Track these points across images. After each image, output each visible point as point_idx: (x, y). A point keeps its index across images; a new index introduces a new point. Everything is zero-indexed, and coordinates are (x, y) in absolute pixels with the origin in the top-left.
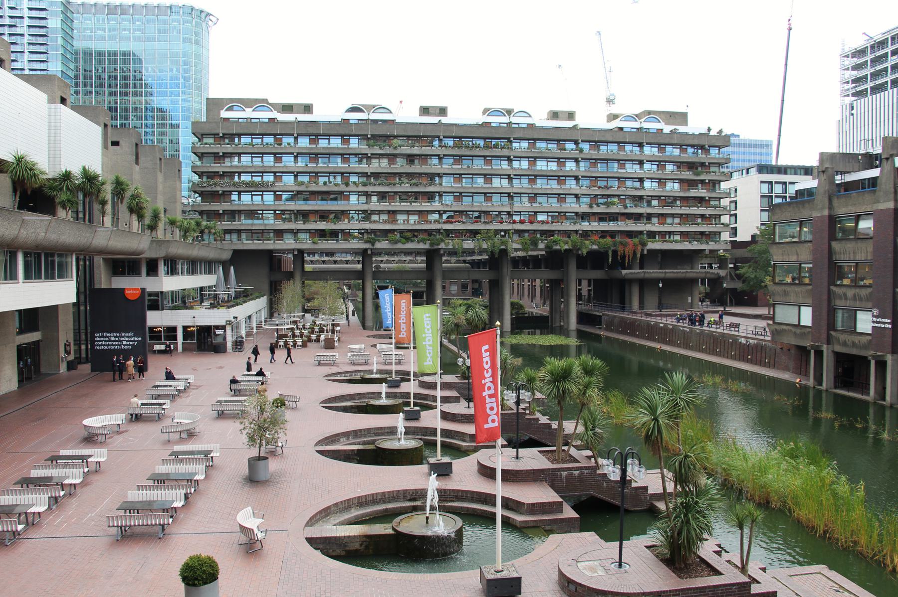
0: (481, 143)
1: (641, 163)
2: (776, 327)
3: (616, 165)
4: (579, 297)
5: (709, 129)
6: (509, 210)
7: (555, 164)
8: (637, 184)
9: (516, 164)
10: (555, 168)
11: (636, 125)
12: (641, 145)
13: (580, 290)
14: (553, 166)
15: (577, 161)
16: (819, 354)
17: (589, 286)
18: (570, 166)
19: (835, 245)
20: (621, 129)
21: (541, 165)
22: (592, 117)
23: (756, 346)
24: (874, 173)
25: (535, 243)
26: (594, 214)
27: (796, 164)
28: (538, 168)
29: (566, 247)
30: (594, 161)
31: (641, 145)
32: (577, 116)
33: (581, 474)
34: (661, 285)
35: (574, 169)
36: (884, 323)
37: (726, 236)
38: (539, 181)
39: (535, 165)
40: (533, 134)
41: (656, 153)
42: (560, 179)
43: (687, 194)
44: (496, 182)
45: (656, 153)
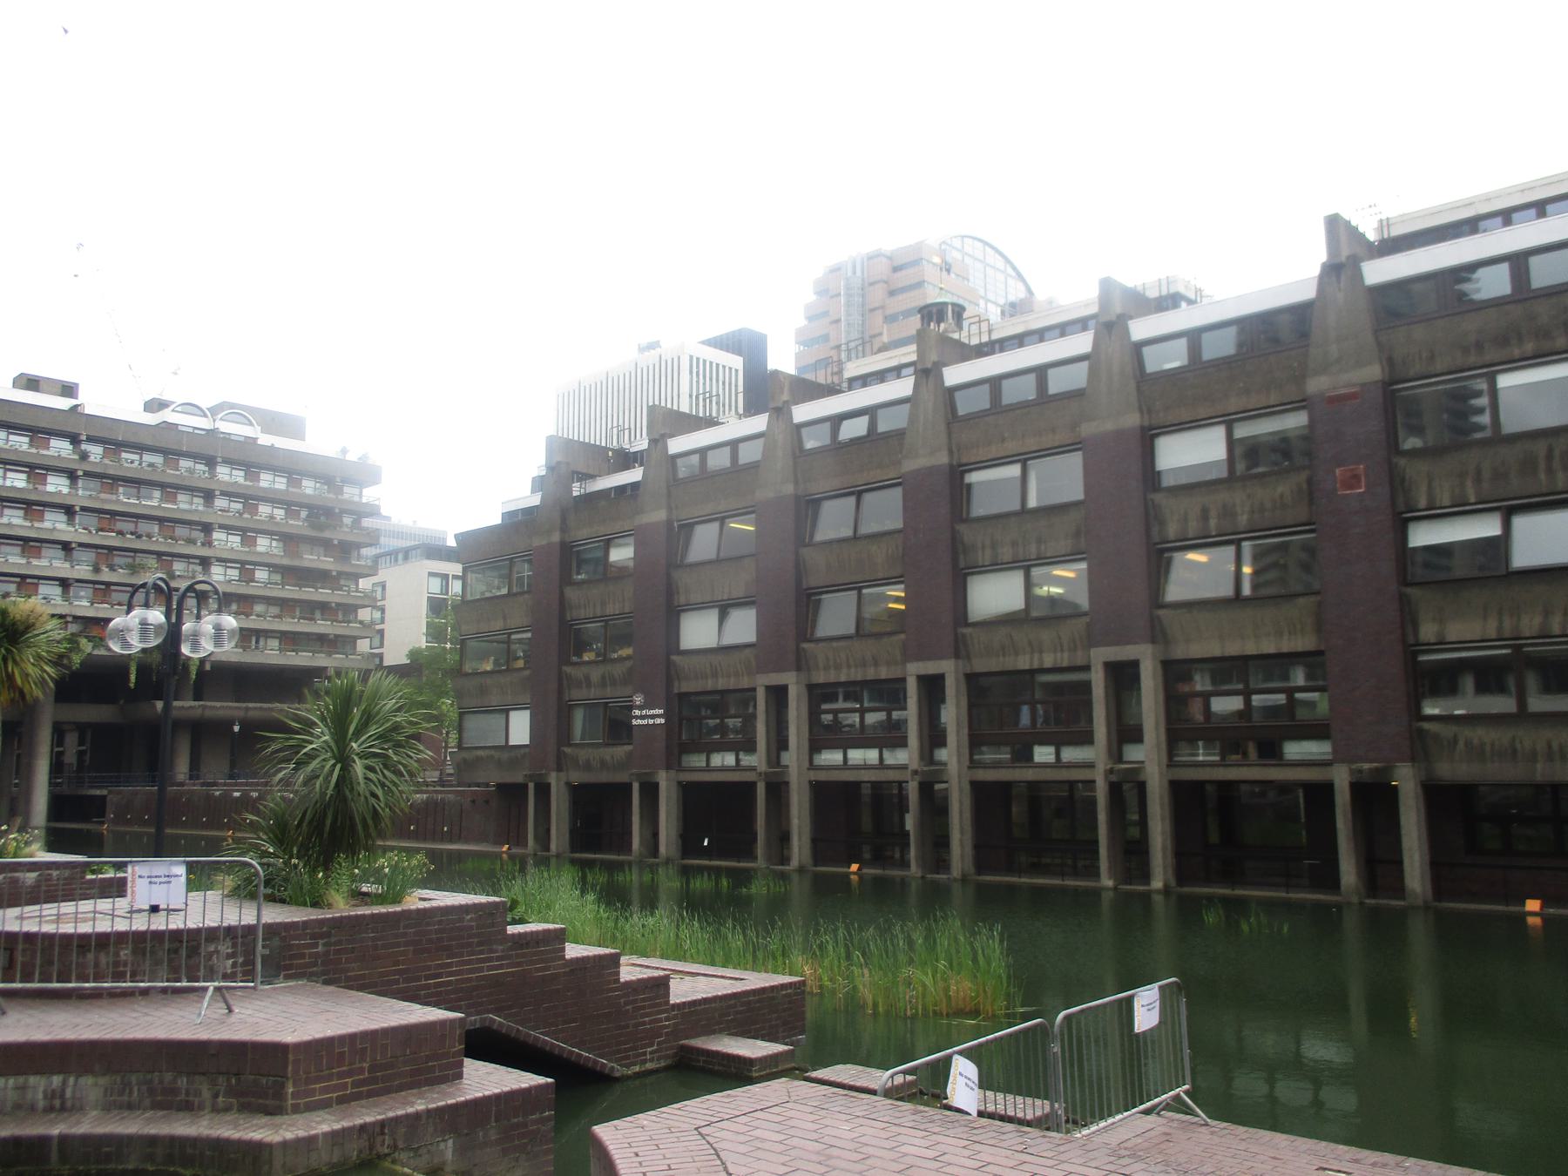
1: (208, 496)
2: (465, 755)
4: (57, 767)
5: (344, 451)
8: (199, 536)
11: (204, 423)
12: (211, 462)
13: (60, 754)
15: (72, 476)
16: (543, 790)
17: (81, 742)
18: (56, 485)
22: (111, 397)
23: (427, 803)
30: (111, 481)
31: (211, 462)
34: (236, 729)
35: (65, 490)
36: (653, 717)
37: (363, 646)
41: (241, 480)
43: (296, 563)
45: (241, 480)
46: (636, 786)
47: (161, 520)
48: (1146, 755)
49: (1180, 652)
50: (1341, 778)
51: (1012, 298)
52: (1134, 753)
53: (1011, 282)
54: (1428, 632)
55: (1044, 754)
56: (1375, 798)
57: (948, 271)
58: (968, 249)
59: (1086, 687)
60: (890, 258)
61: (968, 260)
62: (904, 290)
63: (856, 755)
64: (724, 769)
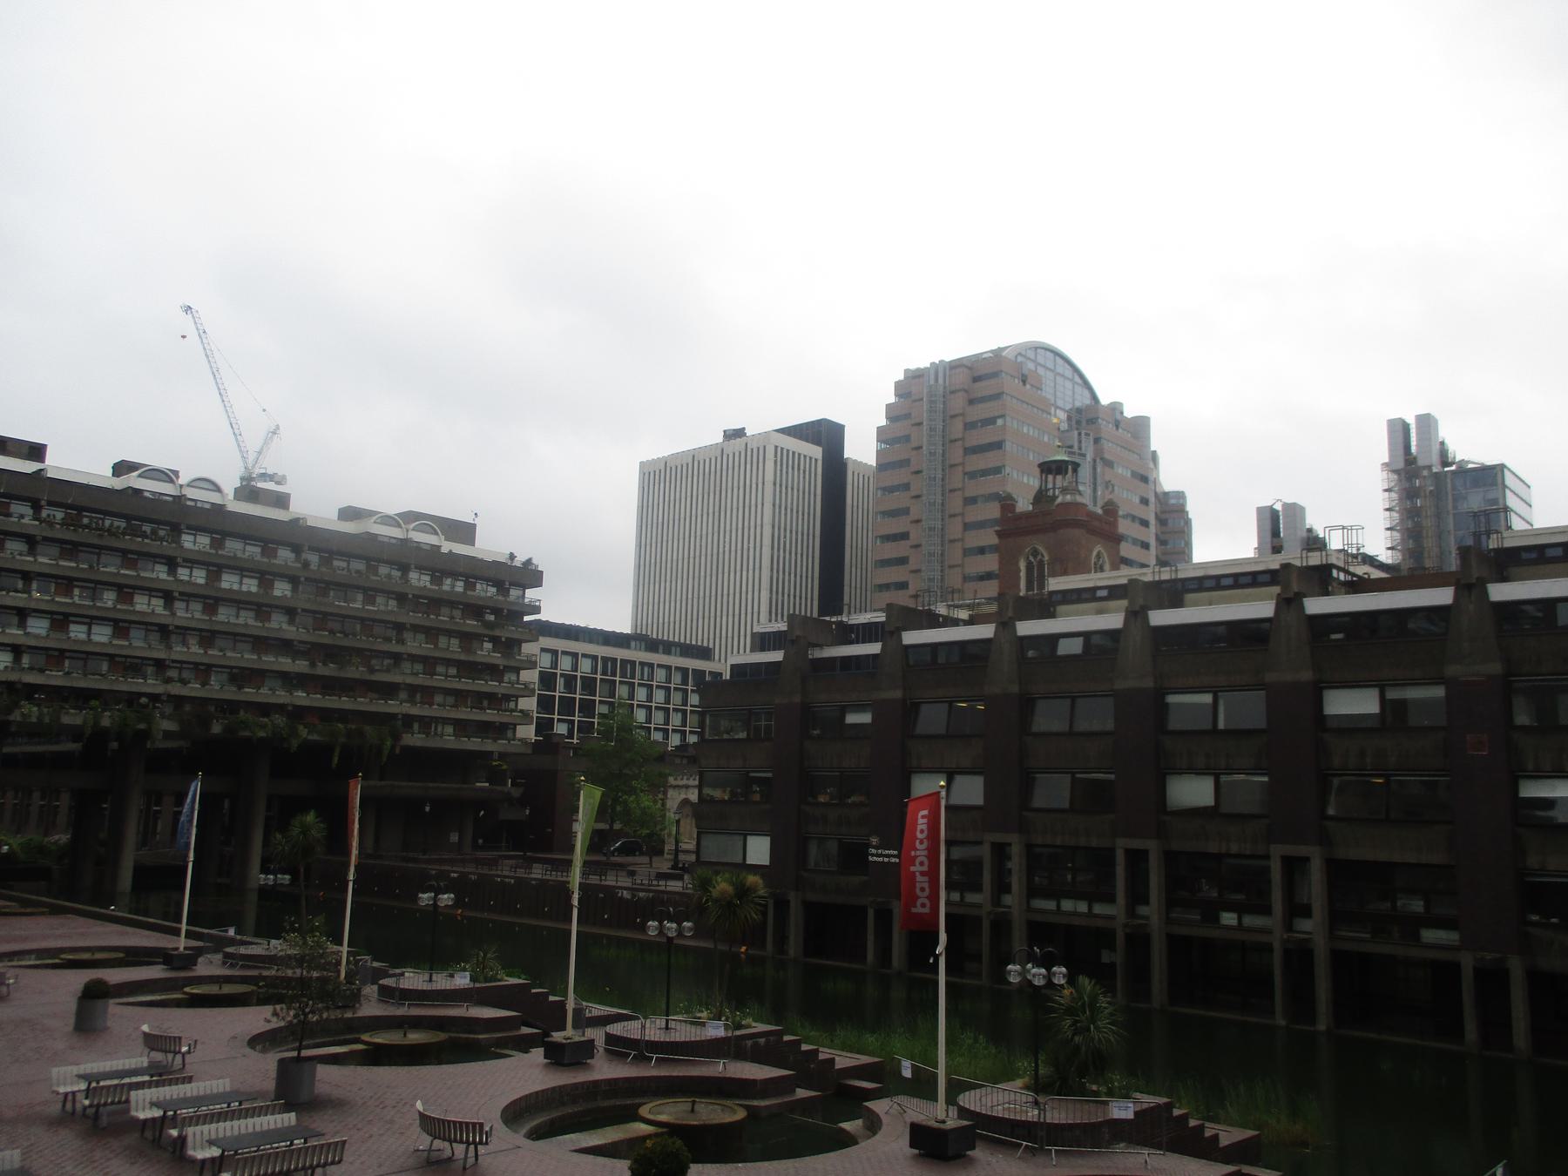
3: (360, 597)
6: (162, 655)
7: (255, 582)
8: (392, 633)
9: (183, 573)
10: (254, 589)
11: (396, 533)
15: (294, 581)
18: (281, 589)
21: (229, 582)
24: (874, 648)
27: (594, 624)
28: (225, 585)
29: (262, 734)
33: (767, 1042)
35: (289, 594)
39: (220, 580)
42: (262, 609)
44: (141, 603)
46: (871, 913)
47: (362, 620)
48: (1311, 927)
50: (1467, 961)
51: (1078, 404)
52: (1305, 925)
53: (1079, 389)
55: (1229, 918)
56: (1492, 981)
57: (1024, 382)
58: (1040, 360)
59: (1267, 870)
60: (970, 369)
61: (1041, 371)
62: (983, 400)
63: (1067, 905)
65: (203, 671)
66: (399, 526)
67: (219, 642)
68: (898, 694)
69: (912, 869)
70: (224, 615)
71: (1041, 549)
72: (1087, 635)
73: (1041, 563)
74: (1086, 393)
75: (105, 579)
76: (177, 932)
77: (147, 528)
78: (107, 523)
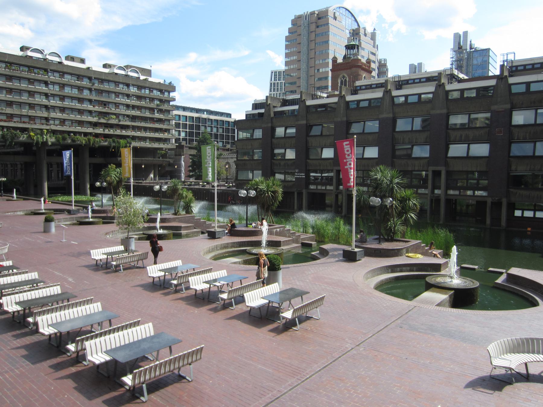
0: (27, 69)
3: (113, 95)
7: (77, 90)
9: (51, 87)
14: (75, 92)
15: (90, 90)
18: (86, 93)
19: (273, 140)
20: (116, 74)
21: (67, 90)
24: (296, 107)
25: (64, 139)
26: (101, 123)
31: (128, 85)
32: (86, 61)
34: (143, 166)
38: (66, 100)
40: (61, 70)
46: (296, 194)
49: (451, 169)
54: (513, 168)
64: (321, 189)
65: (63, 122)
66: (125, 70)
67: (67, 112)
68: (304, 122)
69: (346, 167)
70: (67, 103)
71: (346, 75)
72: (370, 100)
73: (346, 80)
74: (356, 24)
75: (23, 88)
76: (72, 205)
77: (36, 71)
78: (21, 68)
